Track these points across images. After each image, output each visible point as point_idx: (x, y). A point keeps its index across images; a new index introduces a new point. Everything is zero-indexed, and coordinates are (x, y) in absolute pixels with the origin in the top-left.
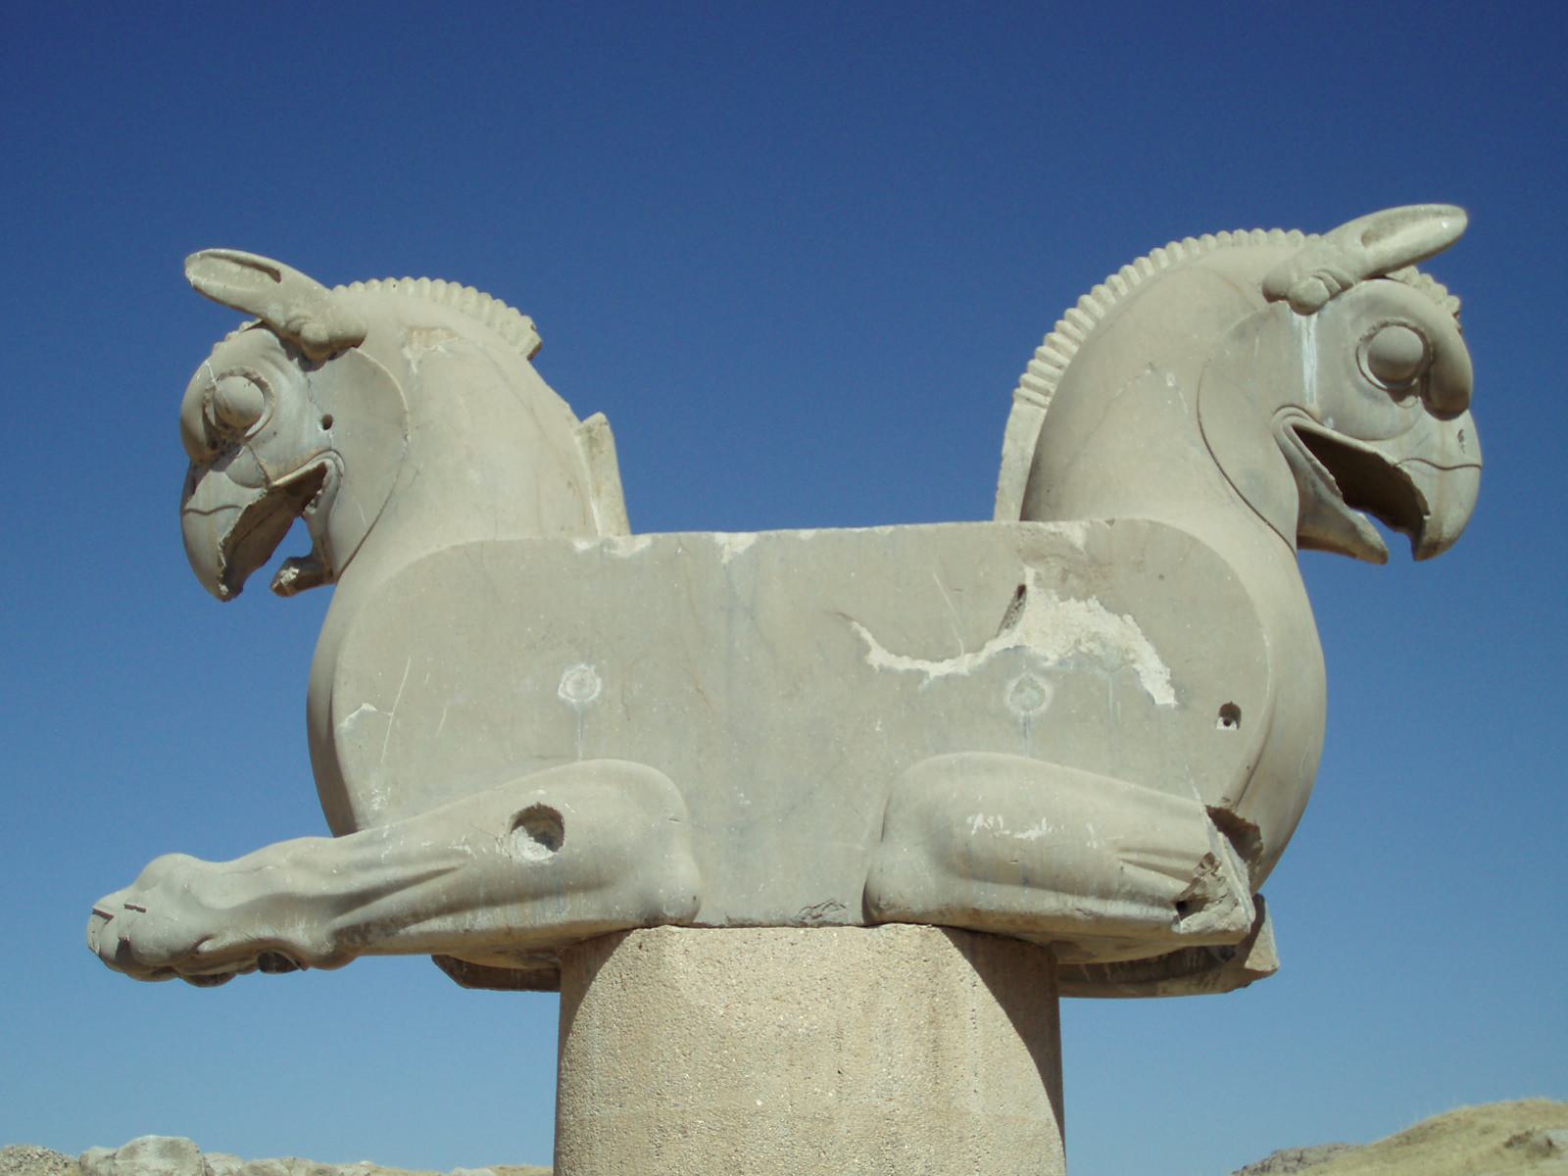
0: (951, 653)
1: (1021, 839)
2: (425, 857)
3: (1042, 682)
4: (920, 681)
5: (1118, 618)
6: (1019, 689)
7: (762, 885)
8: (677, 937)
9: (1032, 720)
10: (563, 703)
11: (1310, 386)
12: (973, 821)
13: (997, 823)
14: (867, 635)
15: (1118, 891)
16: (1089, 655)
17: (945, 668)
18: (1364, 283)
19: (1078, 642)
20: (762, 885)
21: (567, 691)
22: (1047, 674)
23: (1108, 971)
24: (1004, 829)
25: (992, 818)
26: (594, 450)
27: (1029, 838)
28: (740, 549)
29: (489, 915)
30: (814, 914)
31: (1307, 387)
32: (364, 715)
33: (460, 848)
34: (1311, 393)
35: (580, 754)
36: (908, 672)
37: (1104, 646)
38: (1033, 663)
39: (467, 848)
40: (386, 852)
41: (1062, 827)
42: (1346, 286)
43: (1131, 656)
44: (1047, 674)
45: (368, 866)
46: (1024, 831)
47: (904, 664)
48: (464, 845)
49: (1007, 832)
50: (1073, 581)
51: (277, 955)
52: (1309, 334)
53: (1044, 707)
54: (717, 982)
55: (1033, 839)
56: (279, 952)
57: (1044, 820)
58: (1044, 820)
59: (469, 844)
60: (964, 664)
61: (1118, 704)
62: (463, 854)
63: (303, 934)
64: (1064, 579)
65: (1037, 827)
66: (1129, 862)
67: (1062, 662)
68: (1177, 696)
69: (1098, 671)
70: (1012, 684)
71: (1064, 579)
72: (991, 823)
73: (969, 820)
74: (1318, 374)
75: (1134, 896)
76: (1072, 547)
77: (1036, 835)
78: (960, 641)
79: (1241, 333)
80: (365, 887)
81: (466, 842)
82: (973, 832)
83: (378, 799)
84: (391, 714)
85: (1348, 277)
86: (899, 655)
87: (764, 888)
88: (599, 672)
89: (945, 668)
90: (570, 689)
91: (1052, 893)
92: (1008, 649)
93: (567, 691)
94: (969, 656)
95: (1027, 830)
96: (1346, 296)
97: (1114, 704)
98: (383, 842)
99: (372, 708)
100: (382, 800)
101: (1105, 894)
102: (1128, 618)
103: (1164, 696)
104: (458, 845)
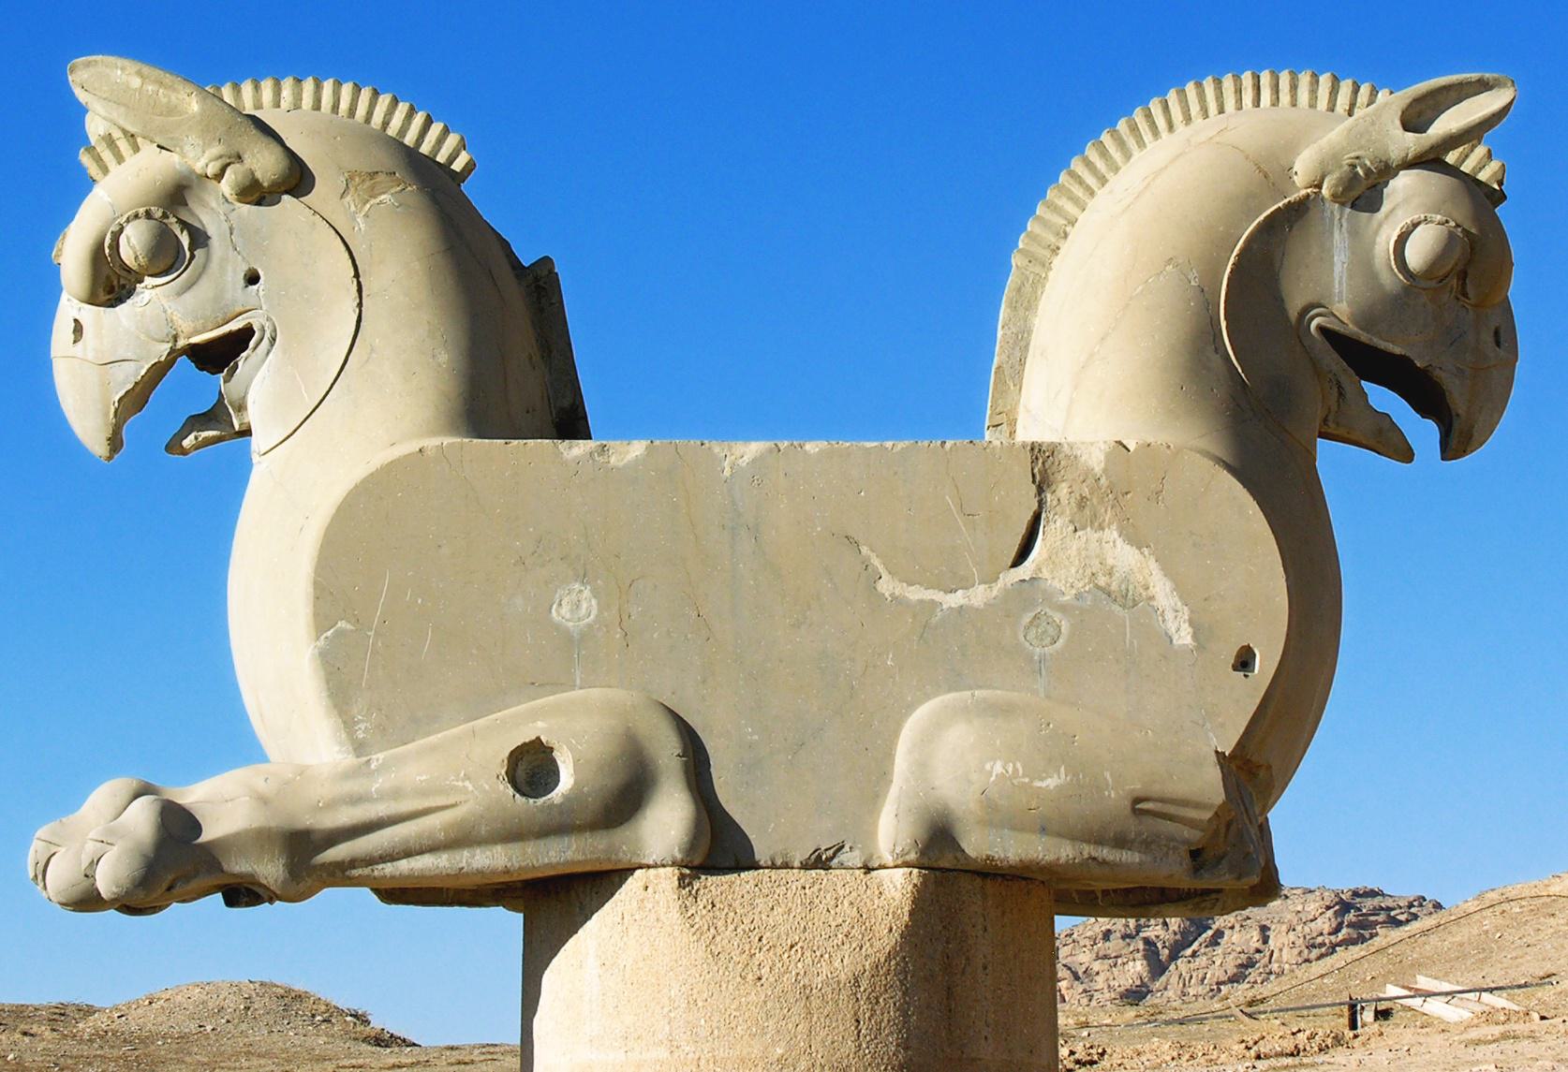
0: (966, 584)
1: (1040, 788)
2: (424, 793)
3: (1057, 617)
5: (1137, 551)
7: (773, 825)
9: (1048, 657)
10: (557, 627)
11: (1340, 283)
12: (992, 768)
13: (1015, 770)
14: (876, 562)
15: (1132, 842)
20: (773, 825)
21: (561, 613)
22: (1063, 608)
23: (1099, 895)
24: (1024, 776)
25: (1011, 765)
26: (543, 300)
27: (1048, 786)
29: (488, 853)
31: (1337, 286)
32: (341, 633)
33: (460, 784)
34: (1340, 292)
35: (578, 682)
36: (921, 602)
38: (1048, 597)
40: (378, 784)
41: (1081, 776)
44: (1063, 608)
45: (355, 800)
46: (1042, 779)
47: (916, 594)
48: (463, 781)
49: (1027, 780)
51: (247, 889)
55: (1052, 787)
56: (251, 887)
57: (1062, 769)
58: (1062, 769)
59: (469, 779)
60: (978, 596)
61: (1135, 642)
65: (1056, 776)
67: (1078, 596)
68: (1195, 637)
70: (1027, 618)
72: (1010, 770)
74: (1349, 270)
77: (1055, 784)
78: (974, 569)
80: (355, 821)
81: (467, 777)
82: (993, 779)
83: (362, 726)
84: (371, 633)
86: (911, 584)
87: (774, 828)
88: (595, 594)
90: (565, 610)
92: (1024, 580)
93: (561, 613)
94: (982, 587)
95: (1046, 778)
97: (1132, 643)
98: (371, 774)
99: (349, 627)
100: (366, 728)
103: (1184, 637)
104: (457, 781)
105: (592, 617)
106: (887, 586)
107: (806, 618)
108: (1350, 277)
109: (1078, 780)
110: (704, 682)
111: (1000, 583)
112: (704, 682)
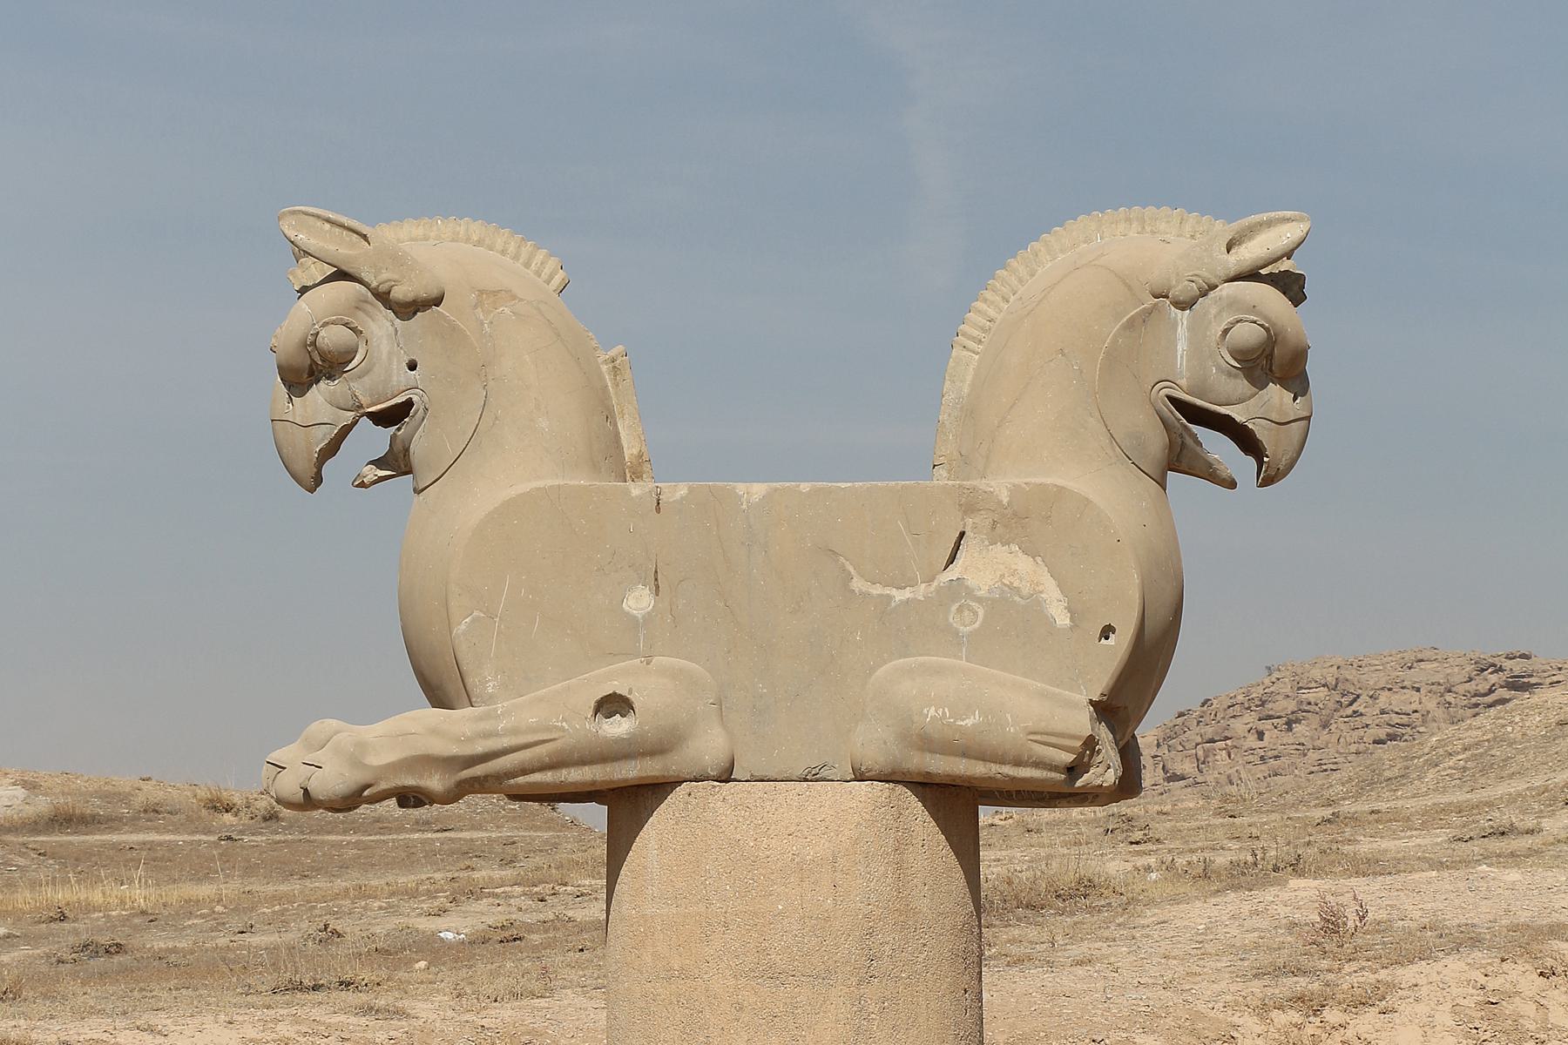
2: (534, 730)
4: (889, 603)
6: (960, 610)
8: (717, 789)
13: (944, 713)
14: (851, 569)
15: (1027, 761)
16: (1011, 587)
17: (906, 594)
18: (1226, 284)
19: (1002, 576)
22: (979, 600)
28: (756, 498)
30: (813, 772)
37: (1021, 579)
38: (970, 593)
39: (564, 724)
42: (1213, 287)
43: (1041, 588)
44: (979, 600)
47: (877, 590)
50: (1000, 529)
52: (1182, 324)
53: (977, 625)
54: (748, 822)
62: (562, 729)
63: (435, 782)
64: (993, 528)
65: (972, 717)
66: (1036, 741)
67: (990, 591)
68: (1072, 619)
69: (1017, 598)
71: (993, 528)
73: (925, 711)
75: (1037, 764)
76: (1000, 502)
79: (1130, 325)
81: (564, 720)
84: (497, 619)
85: (1214, 281)
89: (906, 594)
91: (981, 762)
96: (1212, 294)
100: (494, 685)
101: (1018, 763)
102: (1039, 559)
105: (651, 607)
106: (858, 584)
107: (800, 607)
108: (1188, 361)
109: (988, 720)
110: (729, 652)
111: (935, 583)
112: (729, 652)
